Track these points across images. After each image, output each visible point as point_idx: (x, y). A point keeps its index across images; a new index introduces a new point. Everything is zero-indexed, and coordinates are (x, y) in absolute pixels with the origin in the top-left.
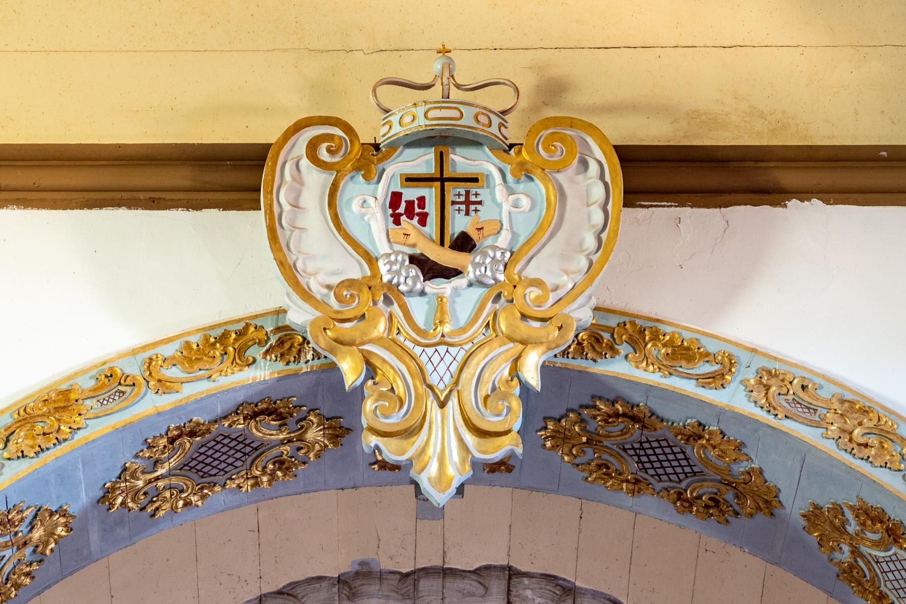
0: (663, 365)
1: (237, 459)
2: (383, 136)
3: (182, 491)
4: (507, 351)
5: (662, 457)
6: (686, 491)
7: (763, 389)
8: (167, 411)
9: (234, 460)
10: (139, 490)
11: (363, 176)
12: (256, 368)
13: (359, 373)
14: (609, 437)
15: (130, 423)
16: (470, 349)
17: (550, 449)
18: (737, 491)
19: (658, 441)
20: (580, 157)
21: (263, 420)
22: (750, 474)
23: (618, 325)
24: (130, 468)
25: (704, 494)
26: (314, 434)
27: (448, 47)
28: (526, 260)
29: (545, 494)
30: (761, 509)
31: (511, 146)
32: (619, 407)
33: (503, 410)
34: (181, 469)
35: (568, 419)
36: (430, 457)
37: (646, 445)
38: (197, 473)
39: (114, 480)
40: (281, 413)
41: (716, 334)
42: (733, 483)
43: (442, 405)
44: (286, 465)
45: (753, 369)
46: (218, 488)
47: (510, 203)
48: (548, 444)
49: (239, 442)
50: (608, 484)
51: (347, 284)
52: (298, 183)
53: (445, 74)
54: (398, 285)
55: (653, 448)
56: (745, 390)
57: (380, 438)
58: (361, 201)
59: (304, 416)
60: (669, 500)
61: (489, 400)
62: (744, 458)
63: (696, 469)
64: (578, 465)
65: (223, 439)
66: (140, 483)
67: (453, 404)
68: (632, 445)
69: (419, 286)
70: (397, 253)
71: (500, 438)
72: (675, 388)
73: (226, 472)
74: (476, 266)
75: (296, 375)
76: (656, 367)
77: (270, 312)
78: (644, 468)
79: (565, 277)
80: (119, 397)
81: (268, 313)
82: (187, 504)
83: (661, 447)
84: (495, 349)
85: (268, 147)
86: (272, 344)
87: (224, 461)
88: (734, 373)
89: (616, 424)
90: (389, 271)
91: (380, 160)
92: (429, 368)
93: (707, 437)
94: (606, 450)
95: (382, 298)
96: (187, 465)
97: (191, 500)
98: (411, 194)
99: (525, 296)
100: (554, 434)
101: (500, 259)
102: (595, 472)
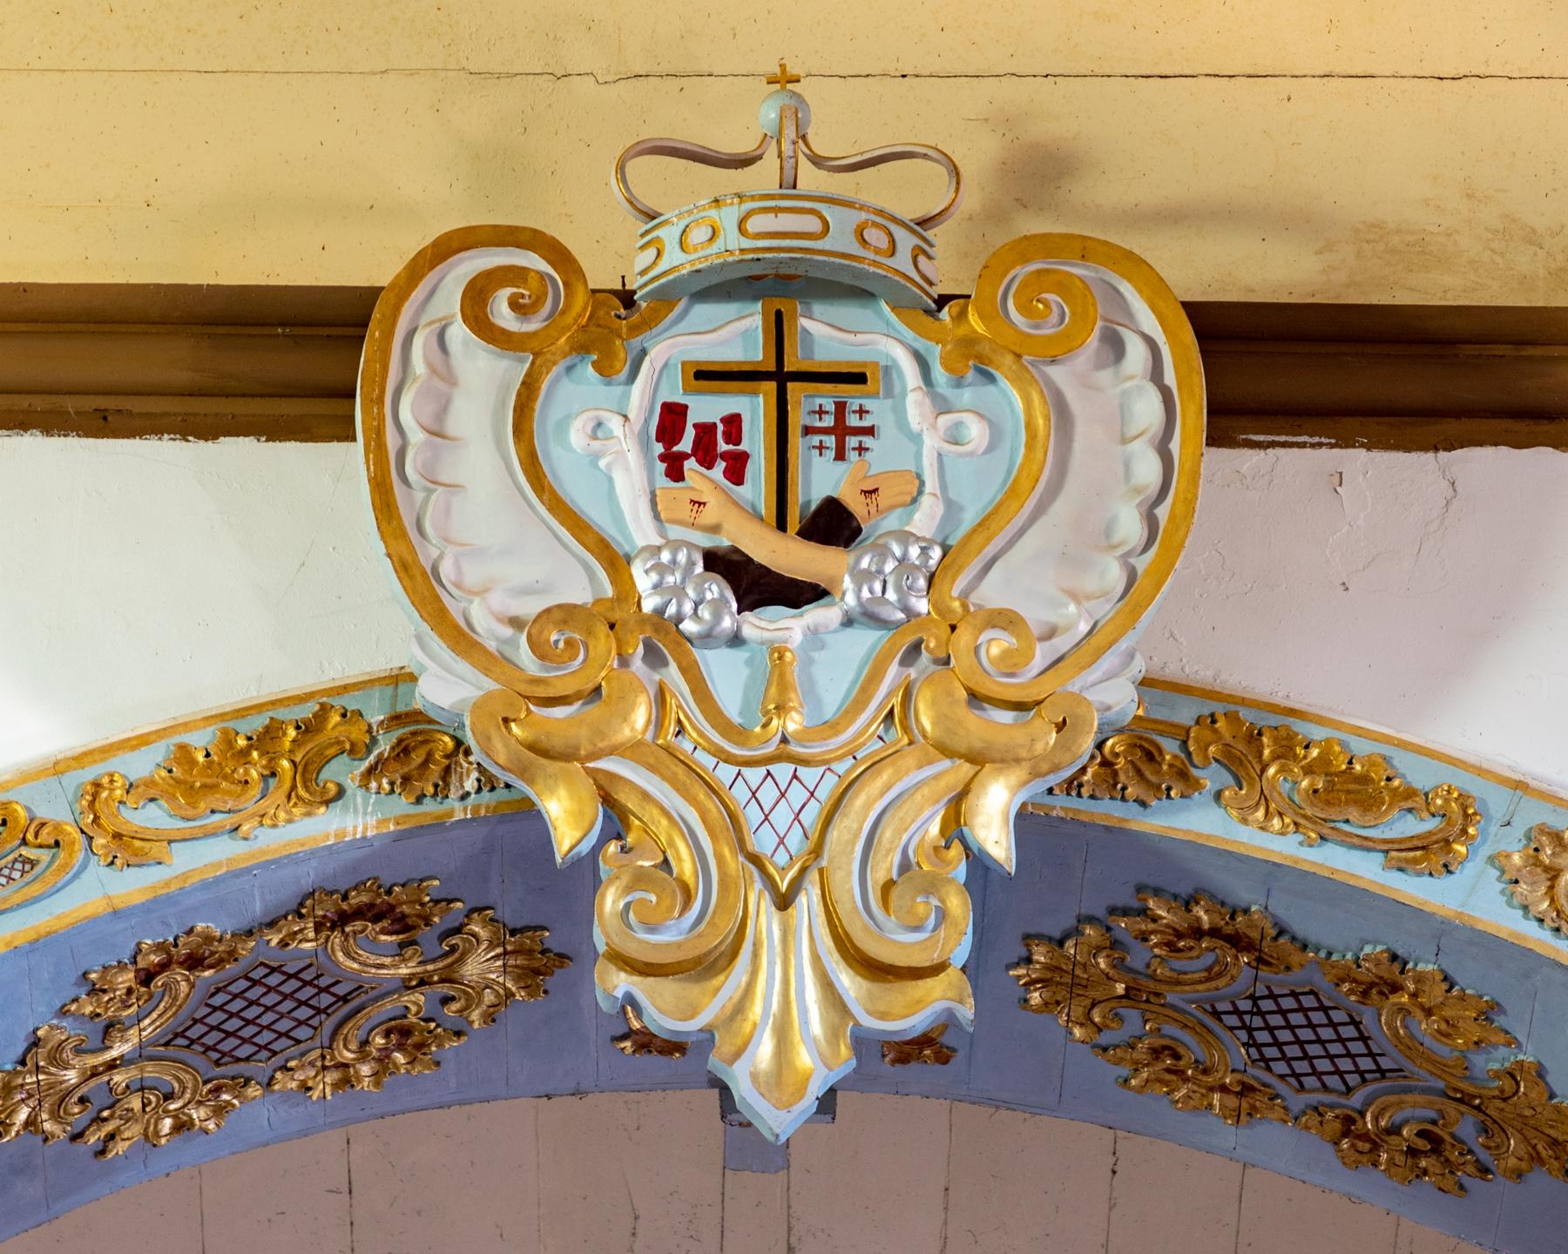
0: (1305, 817)
1: (300, 1023)
2: (643, 273)
3: (169, 1097)
4: (936, 777)
5: (1306, 1034)
6: (1362, 1114)
7: (1544, 876)
8: (135, 907)
9: (294, 1024)
10: (69, 1093)
11: (594, 364)
12: (345, 808)
13: (586, 824)
14: (1178, 983)
15: (49, 933)
16: (849, 771)
17: (1038, 1010)
18: (1482, 1117)
19: (1294, 995)
20: (1106, 328)
21: (362, 932)
22: (1514, 1078)
23: (1198, 722)
24: (47, 1040)
25: (1406, 1122)
26: (479, 966)
27: (793, 69)
28: (980, 566)
29: (1027, 1116)
30: (1542, 1162)
31: (942, 301)
32: (1202, 913)
33: (927, 918)
34: (167, 1044)
35: (1081, 940)
36: (755, 1025)
37: (1267, 1005)
38: (204, 1053)
39: (9, 1067)
40: (404, 916)
41: (1429, 745)
42: (1475, 1097)
43: (784, 902)
44: (415, 1038)
45: (1519, 829)
46: (253, 1091)
47: (941, 432)
48: (1036, 998)
49: (306, 983)
50: (1178, 1095)
51: (558, 615)
52: (443, 379)
53: (786, 132)
54: (679, 619)
55: (1283, 1013)
56: (1499, 879)
57: (637, 979)
58: (591, 425)
59: (457, 924)
60: (1321, 1134)
61: (895, 893)
62: (1501, 1038)
63: (1385, 1063)
64: (1105, 1049)
65: (266, 976)
66: (72, 1076)
67: (808, 901)
68: (1233, 1003)
69: (727, 623)
70: (675, 546)
71: (920, 983)
72: (1334, 870)
73: (275, 1053)
74: (862, 577)
75: (438, 826)
76: (1287, 820)
77: (379, 680)
78: (1263, 1058)
79: (1072, 608)
80: (23, 872)
81: (372, 682)
82: (182, 1126)
83: (1302, 1009)
84: (907, 773)
85: (373, 293)
86: (381, 754)
87: (268, 1027)
88: (1473, 837)
89: (1194, 953)
90: (657, 587)
91: (635, 330)
92: (753, 815)
93: (1412, 987)
94: (1175, 1015)
95: (641, 650)
96: (182, 1034)
97: (190, 1117)
98: (707, 408)
99: (977, 649)
100: (1049, 975)
101: (917, 563)
102: (1147, 1065)
